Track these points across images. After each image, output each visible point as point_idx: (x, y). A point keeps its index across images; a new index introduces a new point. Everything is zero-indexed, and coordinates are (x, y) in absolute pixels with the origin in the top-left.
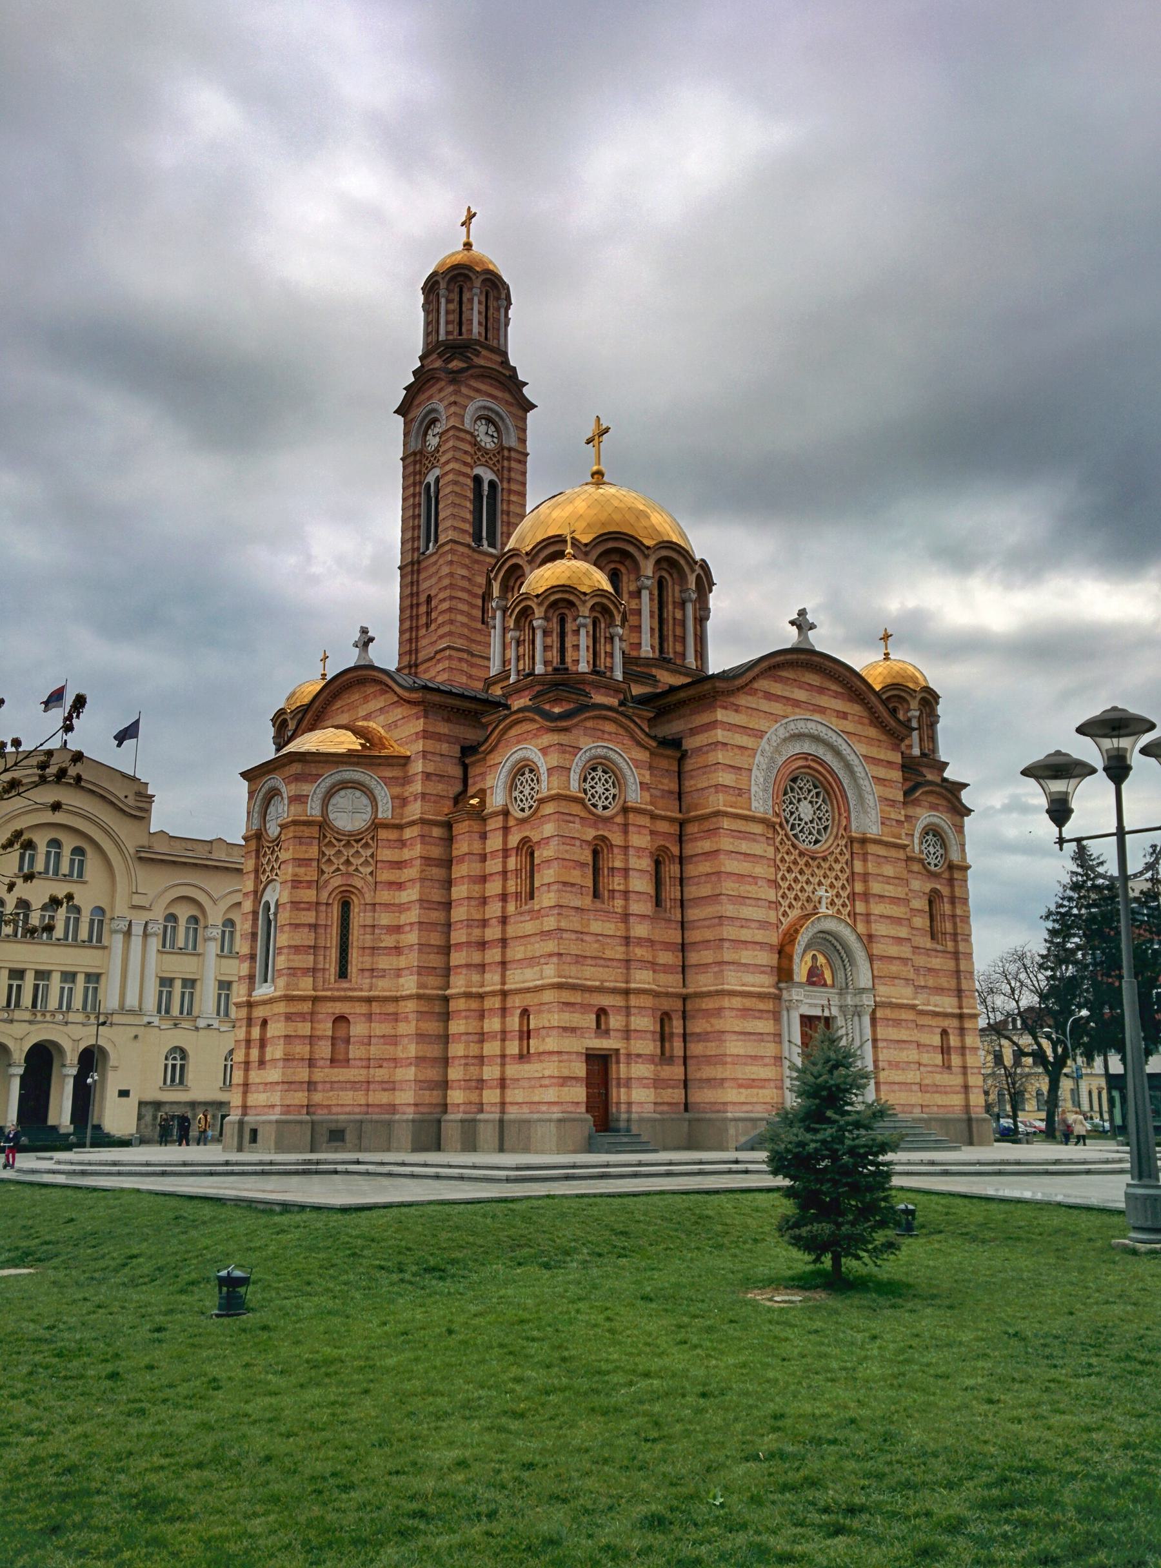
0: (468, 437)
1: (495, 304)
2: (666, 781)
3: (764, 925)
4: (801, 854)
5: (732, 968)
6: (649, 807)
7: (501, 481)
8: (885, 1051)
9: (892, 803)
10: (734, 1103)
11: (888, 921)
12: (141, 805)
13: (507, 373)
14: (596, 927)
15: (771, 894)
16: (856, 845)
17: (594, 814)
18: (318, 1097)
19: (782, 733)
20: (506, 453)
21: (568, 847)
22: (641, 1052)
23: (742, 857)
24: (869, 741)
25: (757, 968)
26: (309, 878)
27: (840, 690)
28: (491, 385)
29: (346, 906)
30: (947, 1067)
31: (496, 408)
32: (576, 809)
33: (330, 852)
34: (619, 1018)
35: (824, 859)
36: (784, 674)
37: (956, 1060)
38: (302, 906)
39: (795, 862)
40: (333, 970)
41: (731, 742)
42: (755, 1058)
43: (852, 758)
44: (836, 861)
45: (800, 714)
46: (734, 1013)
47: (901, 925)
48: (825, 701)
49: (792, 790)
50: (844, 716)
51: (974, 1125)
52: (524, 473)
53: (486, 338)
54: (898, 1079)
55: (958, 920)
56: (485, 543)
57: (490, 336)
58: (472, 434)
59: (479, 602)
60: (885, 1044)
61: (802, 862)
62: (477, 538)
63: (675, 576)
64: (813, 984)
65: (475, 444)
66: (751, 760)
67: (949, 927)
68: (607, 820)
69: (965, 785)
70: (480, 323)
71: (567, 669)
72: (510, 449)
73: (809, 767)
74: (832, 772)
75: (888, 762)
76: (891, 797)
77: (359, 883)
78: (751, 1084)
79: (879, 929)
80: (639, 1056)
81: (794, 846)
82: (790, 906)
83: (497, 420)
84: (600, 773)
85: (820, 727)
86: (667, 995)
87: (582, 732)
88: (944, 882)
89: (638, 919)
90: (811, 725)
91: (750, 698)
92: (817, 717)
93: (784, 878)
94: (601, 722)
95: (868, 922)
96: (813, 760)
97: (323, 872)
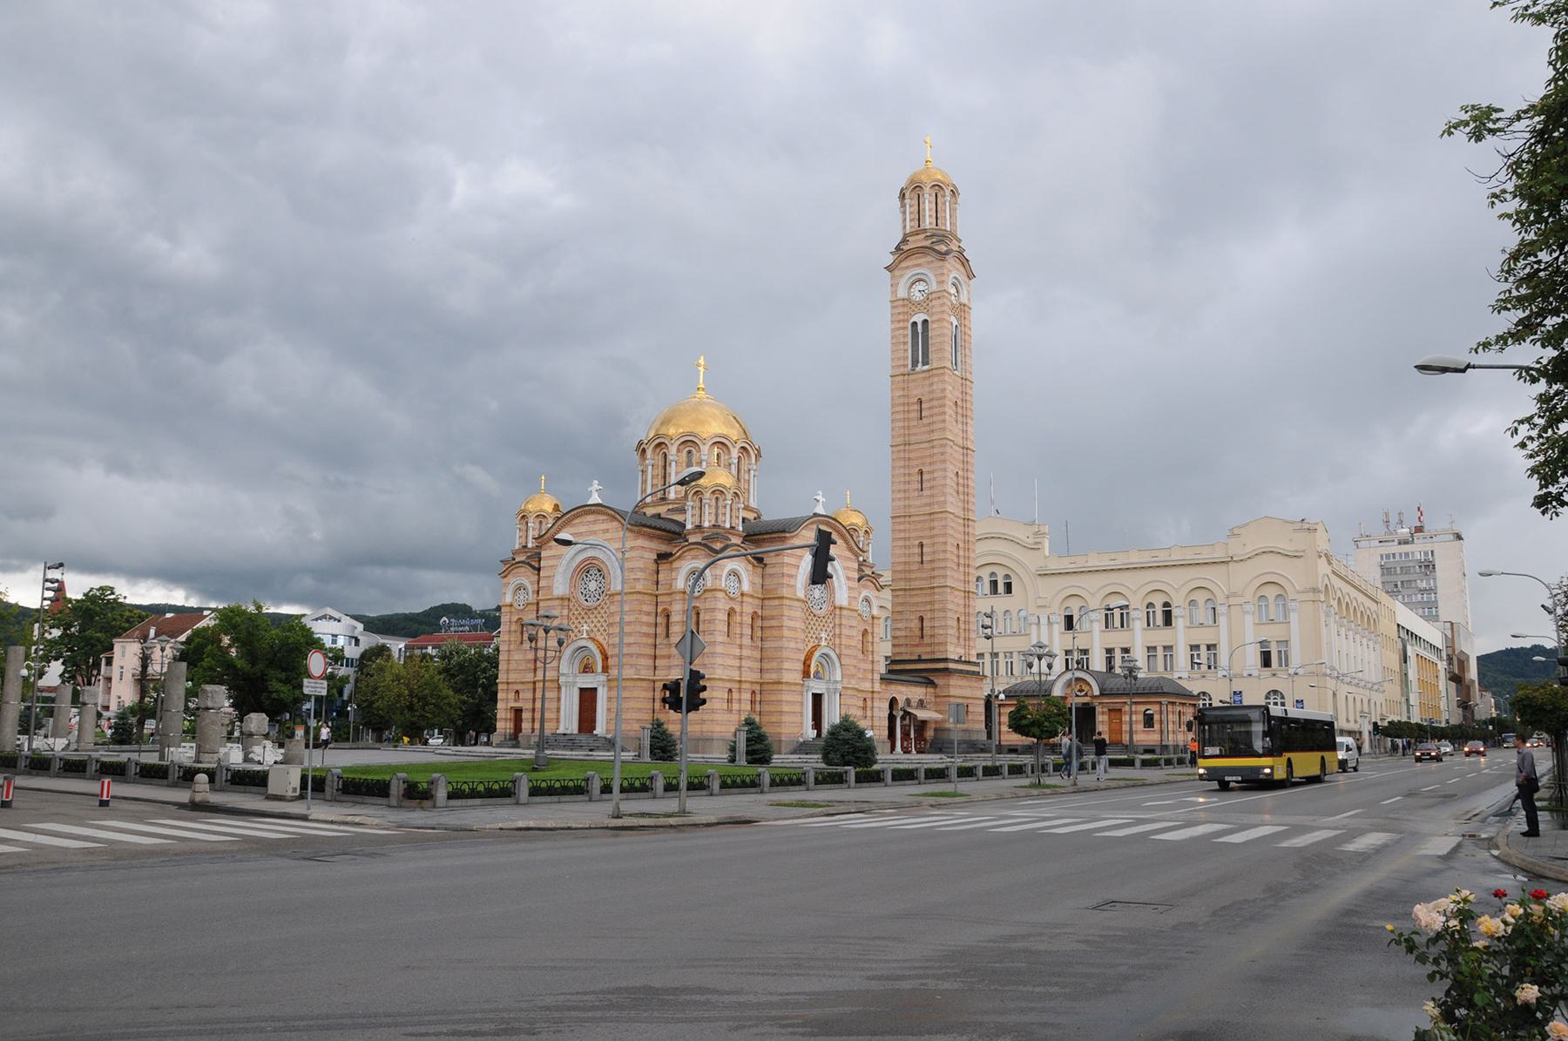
0: (901, 303)
4: (584, 609)
12: (1037, 540)
13: (927, 243)
27: (605, 517)
28: (916, 258)
31: (923, 271)
35: (596, 608)
36: (576, 521)
39: (580, 614)
44: (602, 608)
47: (631, 635)
48: (596, 527)
49: (587, 576)
59: (916, 407)
62: (915, 363)
64: (586, 672)
76: (631, 567)
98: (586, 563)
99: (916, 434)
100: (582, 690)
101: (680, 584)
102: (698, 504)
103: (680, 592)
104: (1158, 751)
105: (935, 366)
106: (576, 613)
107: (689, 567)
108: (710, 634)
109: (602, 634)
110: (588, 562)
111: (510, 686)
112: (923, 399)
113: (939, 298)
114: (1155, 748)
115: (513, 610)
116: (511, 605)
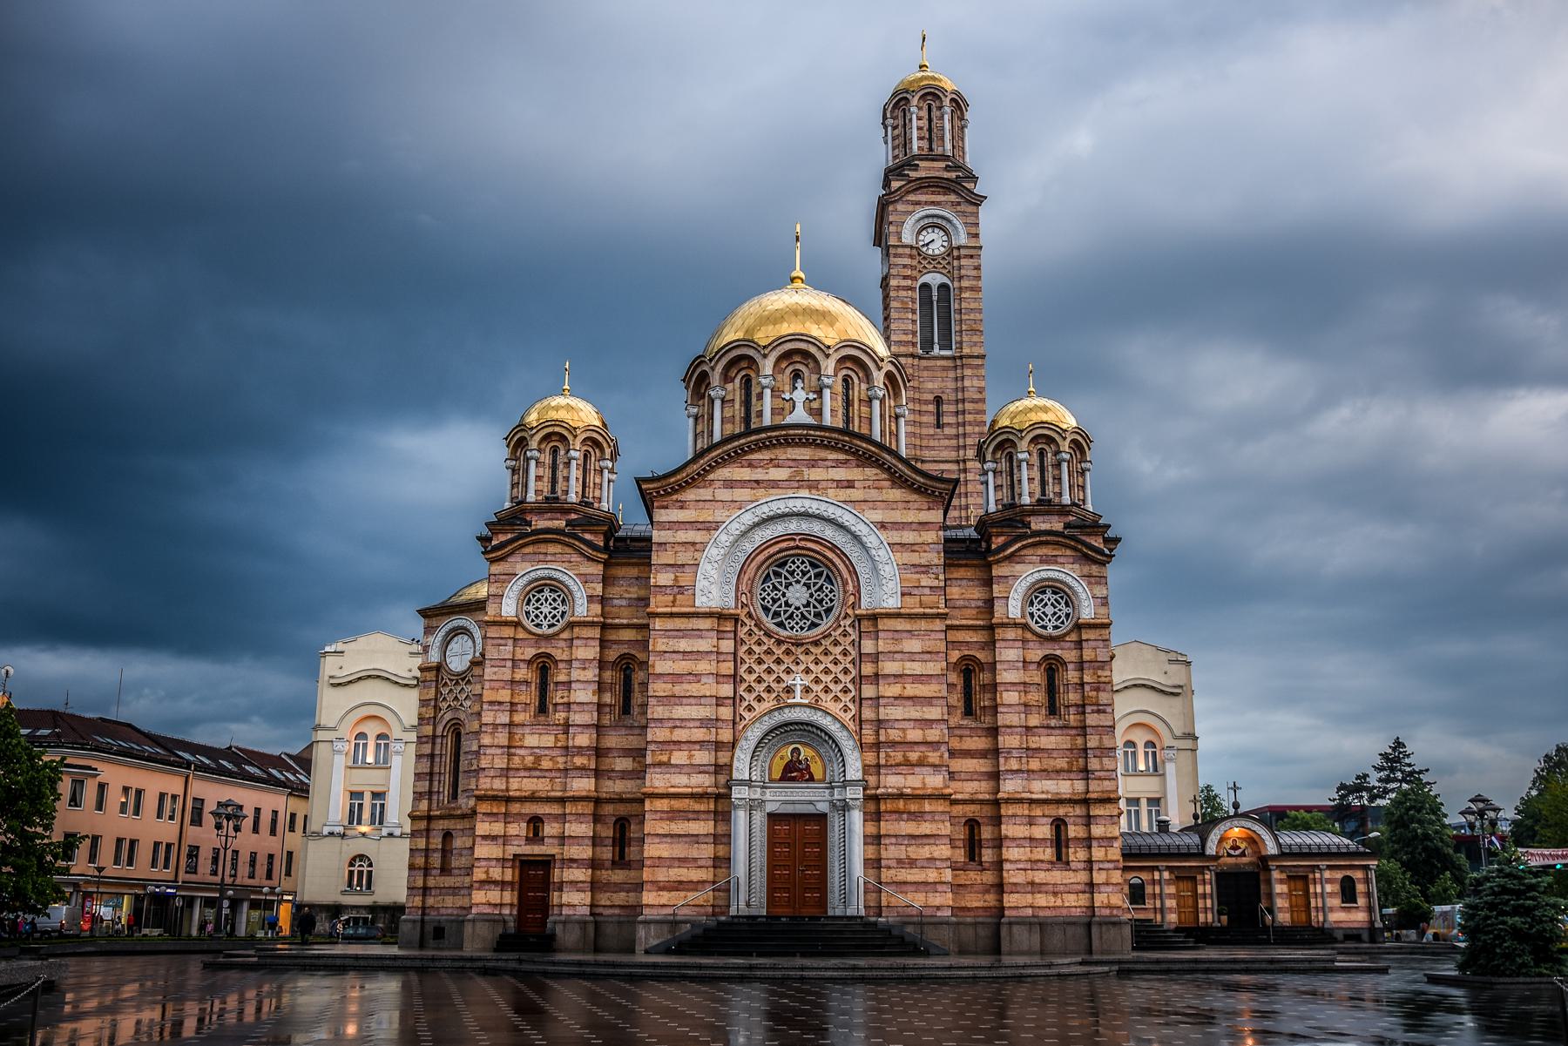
0: (907, 251)
1: (938, 113)
2: (634, 589)
3: (705, 723)
4: (779, 642)
5: (658, 770)
6: (595, 619)
7: (952, 282)
8: (893, 847)
9: (925, 569)
10: (652, 906)
11: (910, 703)
14: (531, 740)
15: (726, 690)
16: (865, 623)
17: (534, 634)
18: (430, 901)
19: (749, 519)
20: (955, 253)
21: (496, 669)
22: (576, 857)
23: (680, 656)
24: (889, 505)
25: (700, 769)
26: (427, 716)
27: (842, 457)
29: (458, 736)
30: (1061, 860)
32: (508, 632)
33: (445, 691)
34: (556, 825)
35: (816, 643)
37: (1077, 855)
38: (424, 739)
39: (769, 652)
40: (446, 792)
41: (672, 540)
42: (683, 861)
43: (860, 529)
44: (836, 643)
45: (775, 493)
46: (658, 816)
48: (815, 474)
50: (850, 484)
51: (1095, 930)
52: (978, 268)
53: (931, 149)
54: (910, 878)
55: (1087, 688)
56: (936, 347)
57: (934, 146)
58: (912, 247)
59: (931, 408)
60: (893, 840)
61: (779, 652)
62: (927, 344)
63: (811, 365)
64: (793, 779)
65: (917, 251)
66: (697, 555)
67: (1073, 697)
68: (548, 638)
69: (1110, 526)
70: (920, 138)
71: (557, 498)
72: (959, 248)
73: (797, 547)
74: (834, 548)
75: (920, 523)
76: (923, 562)
77: (462, 716)
78: (678, 886)
79: (886, 713)
80: (572, 860)
81: (768, 634)
82: (759, 699)
83: (944, 223)
84: (547, 593)
85: (807, 503)
86: (622, 800)
87: (519, 559)
88: (1072, 645)
89: (580, 730)
90: (798, 503)
91: (701, 490)
92: (804, 493)
93: (750, 671)
94: (543, 546)
95: (878, 706)
96: (800, 540)
97: (440, 709)
98: (784, 545)
99: (932, 448)
100: (773, 818)
101: (1014, 609)
102: (1004, 465)
103: (1016, 625)
104: (1365, 936)
105: (966, 351)
106: (755, 648)
107: (1037, 576)
108: (1099, 712)
109: (836, 699)
110: (792, 544)
111: (515, 808)
112: (944, 397)
113: (972, 257)
114: (1361, 931)
115: (521, 635)
116: (517, 624)
